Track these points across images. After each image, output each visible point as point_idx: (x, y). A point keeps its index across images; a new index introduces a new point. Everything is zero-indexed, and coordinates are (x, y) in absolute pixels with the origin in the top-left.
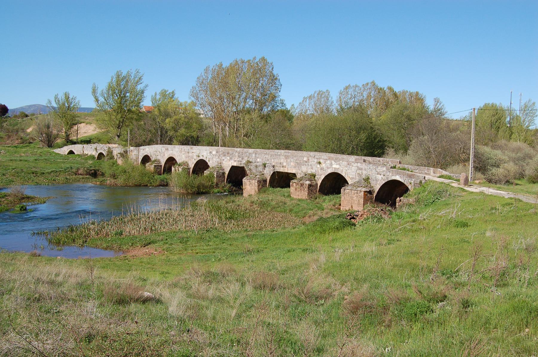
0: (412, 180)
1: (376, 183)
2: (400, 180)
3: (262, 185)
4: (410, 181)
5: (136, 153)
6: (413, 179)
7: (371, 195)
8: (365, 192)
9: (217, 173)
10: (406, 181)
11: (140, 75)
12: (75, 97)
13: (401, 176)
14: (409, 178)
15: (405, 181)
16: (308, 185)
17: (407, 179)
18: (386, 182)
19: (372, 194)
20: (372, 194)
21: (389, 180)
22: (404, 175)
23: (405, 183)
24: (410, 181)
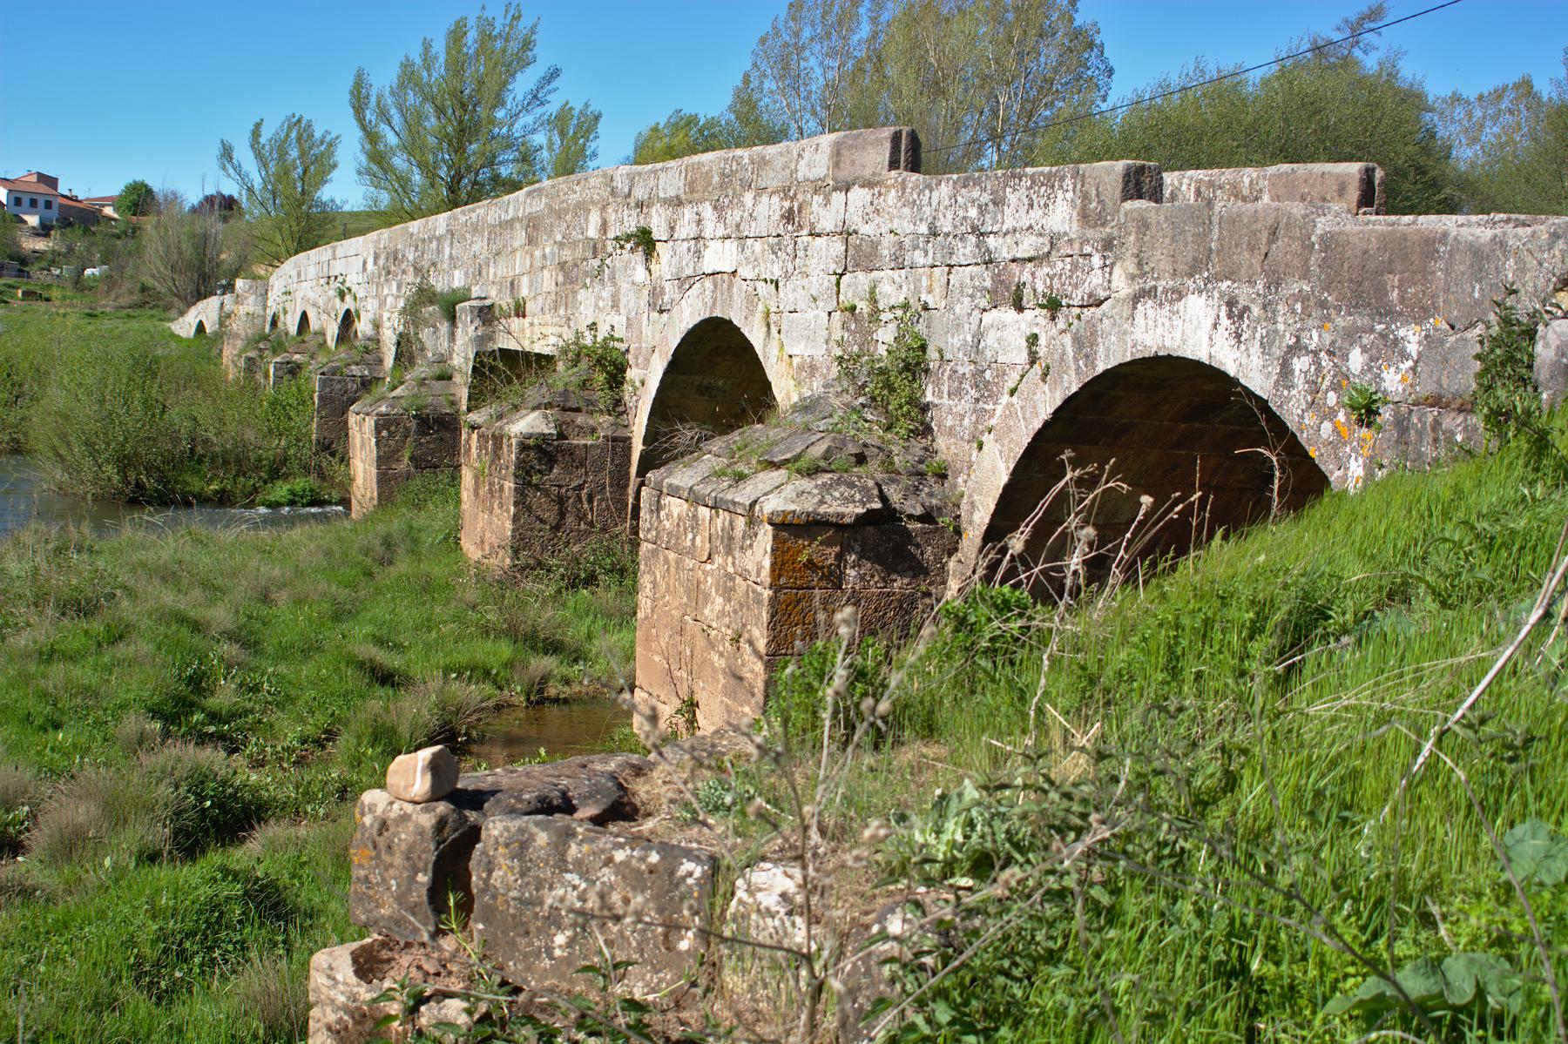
0: (1394, 346)
1: (981, 414)
2: (1228, 359)
3: (412, 459)
4: (1356, 360)
5: (251, 309)
6: (1412, 338)
7: (899, 584)
8: (789, 529)
9: (324, 383)
10: (1300, 364)
11: (523, 26)
12: (333, 135)
13: (1244, 293)
14: (1343, 321)
15: (1286, 372)
16: (523, 447)
17: (1313, 339)
18: (1069, 401)
19: (917, 569)
20: (917, 569)
21: (1100, 368)
22: (1275, 283)
23: (1293, 410)
24: (1356, 360)
